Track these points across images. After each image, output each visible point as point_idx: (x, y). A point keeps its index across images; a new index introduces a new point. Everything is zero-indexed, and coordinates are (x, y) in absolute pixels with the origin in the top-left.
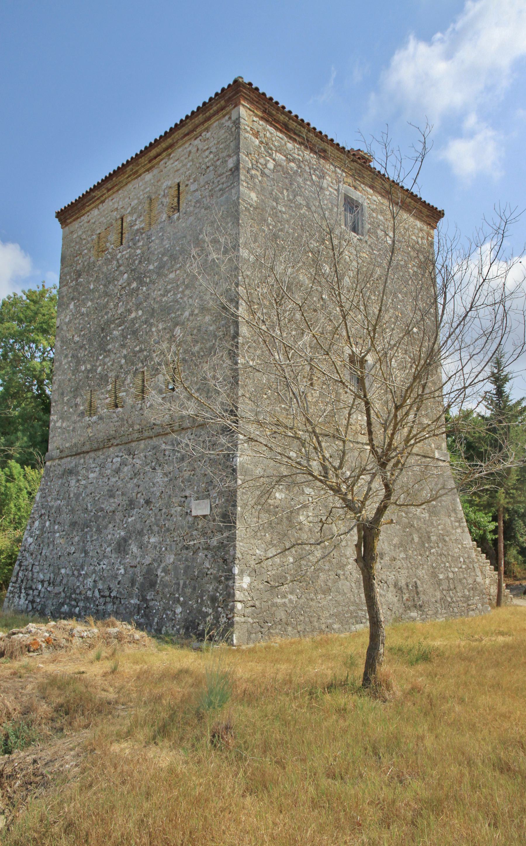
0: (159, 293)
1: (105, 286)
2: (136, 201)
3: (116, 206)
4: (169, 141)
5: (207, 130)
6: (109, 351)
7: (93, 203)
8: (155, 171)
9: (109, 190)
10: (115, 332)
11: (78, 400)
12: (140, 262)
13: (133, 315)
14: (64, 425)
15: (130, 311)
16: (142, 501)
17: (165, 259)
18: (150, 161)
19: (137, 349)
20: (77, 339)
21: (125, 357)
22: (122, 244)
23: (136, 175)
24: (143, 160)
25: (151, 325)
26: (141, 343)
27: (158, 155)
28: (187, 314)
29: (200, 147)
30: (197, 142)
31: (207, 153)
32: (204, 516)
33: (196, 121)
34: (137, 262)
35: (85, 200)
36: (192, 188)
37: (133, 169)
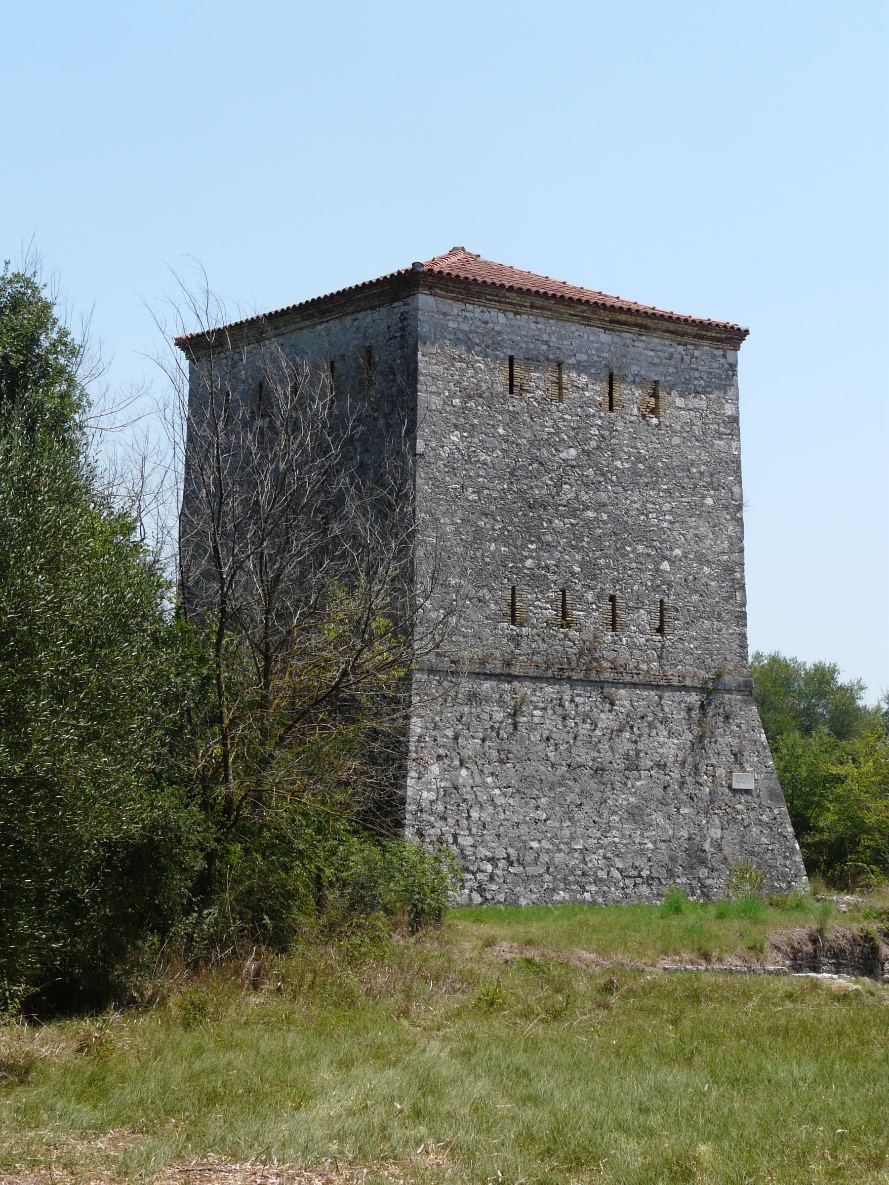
1: (531, 443)
2: (585, 357)
3: (545, 337)
4: (649, 322)
5: (696, 347)
7: (499, 302)
9: (532, 306)
12: (598, 447)
13: (590, 514)
17: (641, 466)
18: (611, 322)
22: (561, 400)
23: (586, 321)
24: (606, 316)
27: (624, 323)
28: (678, 552)
29: (687, 359)
30: (681, 348)
31: (697, 374)
33: (690, 330)
34: (593, 444)
35: (489, 291)
37: (585, 312)
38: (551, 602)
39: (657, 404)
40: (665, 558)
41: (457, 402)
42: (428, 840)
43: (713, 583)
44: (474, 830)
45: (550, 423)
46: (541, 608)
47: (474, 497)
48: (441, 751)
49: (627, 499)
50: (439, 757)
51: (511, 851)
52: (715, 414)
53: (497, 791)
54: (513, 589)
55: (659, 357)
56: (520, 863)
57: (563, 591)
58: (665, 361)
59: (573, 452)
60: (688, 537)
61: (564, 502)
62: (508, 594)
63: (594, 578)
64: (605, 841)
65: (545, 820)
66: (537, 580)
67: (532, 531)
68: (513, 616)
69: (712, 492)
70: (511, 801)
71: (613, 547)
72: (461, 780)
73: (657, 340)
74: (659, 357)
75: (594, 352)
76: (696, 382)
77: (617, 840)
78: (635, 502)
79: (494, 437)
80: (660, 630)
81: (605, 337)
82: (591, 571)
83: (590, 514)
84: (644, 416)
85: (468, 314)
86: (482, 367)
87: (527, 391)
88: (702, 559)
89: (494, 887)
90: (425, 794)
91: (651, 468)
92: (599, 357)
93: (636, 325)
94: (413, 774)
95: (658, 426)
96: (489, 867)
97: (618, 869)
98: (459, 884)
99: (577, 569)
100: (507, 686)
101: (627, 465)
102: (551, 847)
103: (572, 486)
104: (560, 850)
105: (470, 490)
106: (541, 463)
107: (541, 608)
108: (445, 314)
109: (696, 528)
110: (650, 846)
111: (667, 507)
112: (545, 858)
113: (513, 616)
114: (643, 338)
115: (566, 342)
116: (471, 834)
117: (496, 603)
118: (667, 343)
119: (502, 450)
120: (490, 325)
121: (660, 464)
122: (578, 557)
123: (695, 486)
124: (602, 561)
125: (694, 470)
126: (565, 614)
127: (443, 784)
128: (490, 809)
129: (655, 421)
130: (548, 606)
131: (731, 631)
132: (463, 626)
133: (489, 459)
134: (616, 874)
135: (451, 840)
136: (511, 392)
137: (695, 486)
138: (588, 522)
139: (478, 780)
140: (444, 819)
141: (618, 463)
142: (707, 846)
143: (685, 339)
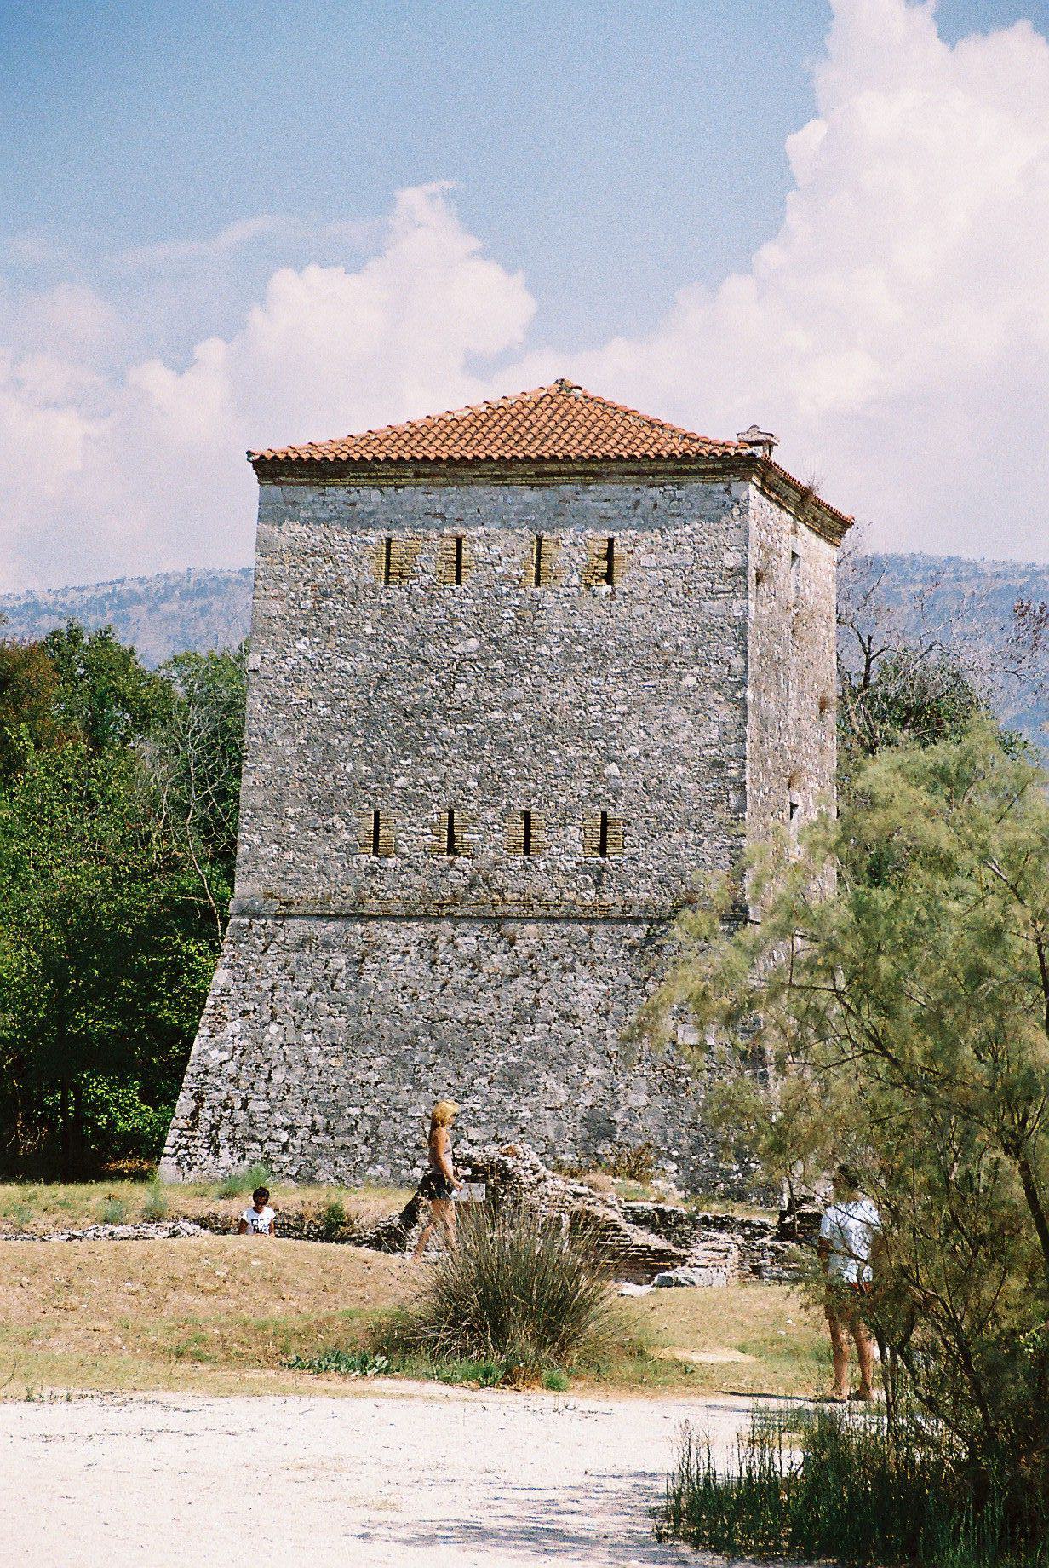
0: (567, 699)
1: (412, 640)
4: (594, 467)
5: (679, 486)
6: (430, 757)
8: (549, 493)
9: (418, 475)
10: (445, 729)
13: (496, 715)
14: (289, 856)
16: (552, 1014)
17: (580, 649)
18: (538, 475)
22: (459, 582)
25: (548, 745)
27: (560, 474)
30: (653, 492)
34: (506, 629)
36: (647, 560)
38: (432, 826)
39: (610, 567)
41: (308, 603)
42: (207, 1105)
43: (690, 786)
44: (273, 1094)
45: (441, 611)
46: (414, 835)
47: (327, 711)
48: (250, 1006)
49: (554, 691)
50: (245, 1013)
51: (318, 1118)
52: (707, 568)
53: (317, 1050)
54: (377, 814)
55: (616, 507)
56: (327, 1131)
57: (451, 813)
58: (625, 512)
59: (474, 643)
60: (652, 731)
61: (457, 705)
62: (370, 823)
63: (498, 792)
66: (412, 801)
67: (408, 745)
68: (376, 845)
69: (696, 669)
70: (333, 1061)
71: (528, 752)
72: (267, 1038)
73: (614, 487)
74: (616, 507)
75: (512, 516)
78: (567, 694)
79: (357, 638)
80: (602, 849)
81: (529, 495)
82: (493, 785)
83: (496, 715)
84: (588, 585)
85: (327, 499)
86: (345, 557)
87: (413, 578)
88: (671, 754)
89: (286, 1159)
90: (214, 1053)
91: (595, 650)
93: (578, 473)
94: (204, 1031)
95: (612, 596)
96: (284, 1136)
98: (239, 1154)
99: (472, 784)
100: (359, 928)
101: (556, 650)
102: (377, 1114)
103: (469, 685)
104: (388, 1117)
105: (321, 703)
106: (425, 662)
107: (414, 835)
108: (294, 503)
109: (666, 717)
110: (529, 1115)
113: (376, 845)
115: (469, 511)
116: (267, 1098)
117: (351, 831)
118: (630, 488)
120: (359, 507)
121: (610, 643)
122: (475, 769)
123: (667, 664)
125: (667, 644)
126: (452, 838)
129: (608, 589)
131: (718, 844)
132: (302, 861)
135: (238, 1105)
137: (667, 664)
138: (492, 727)
139: (291, 1037)
141: (544, 650)
142: (618, 1116)
143: (659, 479)
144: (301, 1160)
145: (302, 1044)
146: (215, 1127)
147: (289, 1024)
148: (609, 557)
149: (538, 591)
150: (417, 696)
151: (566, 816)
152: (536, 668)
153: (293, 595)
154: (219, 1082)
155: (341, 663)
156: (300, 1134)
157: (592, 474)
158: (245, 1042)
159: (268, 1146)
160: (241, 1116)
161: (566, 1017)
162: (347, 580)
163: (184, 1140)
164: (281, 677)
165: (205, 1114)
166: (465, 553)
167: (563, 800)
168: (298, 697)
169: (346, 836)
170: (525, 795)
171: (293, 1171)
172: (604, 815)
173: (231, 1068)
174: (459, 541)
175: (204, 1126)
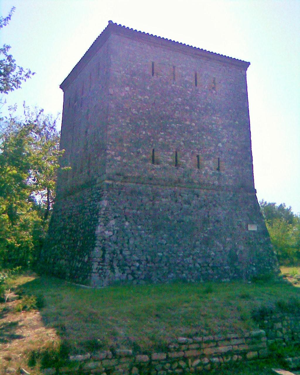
6: (169, 133)
11: (140, 150)
12: (191, 99)
13: (188, 123)
15: (186, 120)
19: (193, 141)
20: (134, 111)
21: (183, 142)
26: (195, 140)
30: (224, 67)
32: (254, 231)
34: (188, 97)
40: (219, 142)
42: (107, 252)
44: (131, 248)
49: (203, 119)
50: (115, 217)
51: (148, 257)
53: (143, 232)
54: (153, 150)
57: (176, 153)
59: (180, 99)
61: (176, 118)
64: (193, 252)
65: (166, 244)
66: (165, 147)
70: (150, 236)
76: (231, 80)
77: (198, 252)
80: (218, 169)
86: (140, 64)
89: (139, 273)
90: (107, 232)
92: (190, 66)
95: (216, 94)
96: (138, 264)
97: (199, 264)
111: (220, 123)
112: (165, 259)
114: (209, 62)
119: (148, 96)
124: (193, 141)
127: (116, 228)
128: (139, 239)
129: (214, 92)
130: (169, 157)
131: (248, 171)
133: (143, 98)
134: (198, 266)
135: (119, 252)
136: (153, 75)
140: (116, 243)
141: (200, 106)
144: (145, 273)
145: (138, 230)
146: (111, 261)
147: (132, 222)
148: (214, 82)
149: (197, 88)
150: (164, 113)
151: (208, 158)
152: (198, 111)
153: (124, 72)
154: (110, 243)
155: (140, 97)
156: (143, 263)
157: (210, 59)
158: (117, 228)
159: (132, 268)
160: (120, 257)
161: (217, 221)
162: (141, 71)
163: (101, 267)
164: (120, 99)
165: (107, 256)
166: (176, 71)
167: (208, 153)
168: (126, 106)
169: (144, 156)
170: (197, 149)
171: (143, 277)
172: (219, 159)
173: (114, 238)
174: (174, 67)
175: (107, 261)
